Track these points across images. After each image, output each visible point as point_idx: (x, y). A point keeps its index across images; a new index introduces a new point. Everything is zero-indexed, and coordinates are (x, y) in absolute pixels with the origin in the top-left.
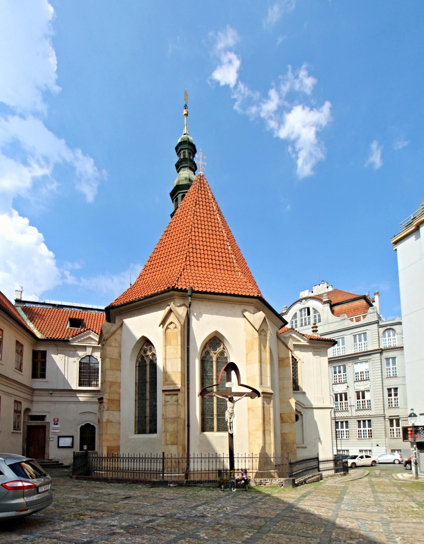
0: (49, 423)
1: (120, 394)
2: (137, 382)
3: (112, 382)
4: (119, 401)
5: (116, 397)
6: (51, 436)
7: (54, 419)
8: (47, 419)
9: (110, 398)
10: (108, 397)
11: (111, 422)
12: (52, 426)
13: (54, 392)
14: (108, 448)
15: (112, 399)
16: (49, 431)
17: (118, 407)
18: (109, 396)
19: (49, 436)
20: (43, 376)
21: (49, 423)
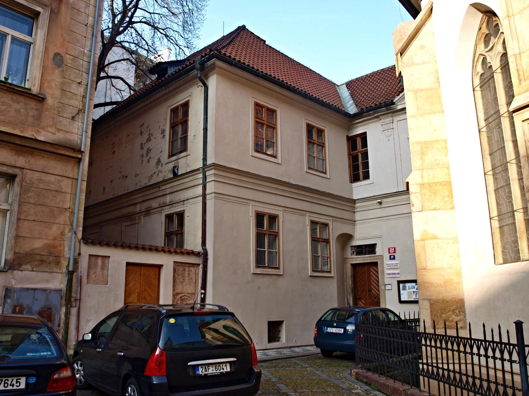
0: (381, 257)
1: (448, 168)
2: (483, 124)
3: (426, 142)
4: (449, 183)
5: (440, 176)
6: (387, 281)
7: (389, 249)
8: (379, 250)
9: (426, 181)
10: (420, 181)
11: (435, 238)
12: (387, 261)
13: (385, 200)
14: (432, 305)
15: (432, 181)
16: (383, 272)
17: (447, 199)
18: (422, 177)
19: (384, 281)
20: (367, 176)
21: (381, 257)
